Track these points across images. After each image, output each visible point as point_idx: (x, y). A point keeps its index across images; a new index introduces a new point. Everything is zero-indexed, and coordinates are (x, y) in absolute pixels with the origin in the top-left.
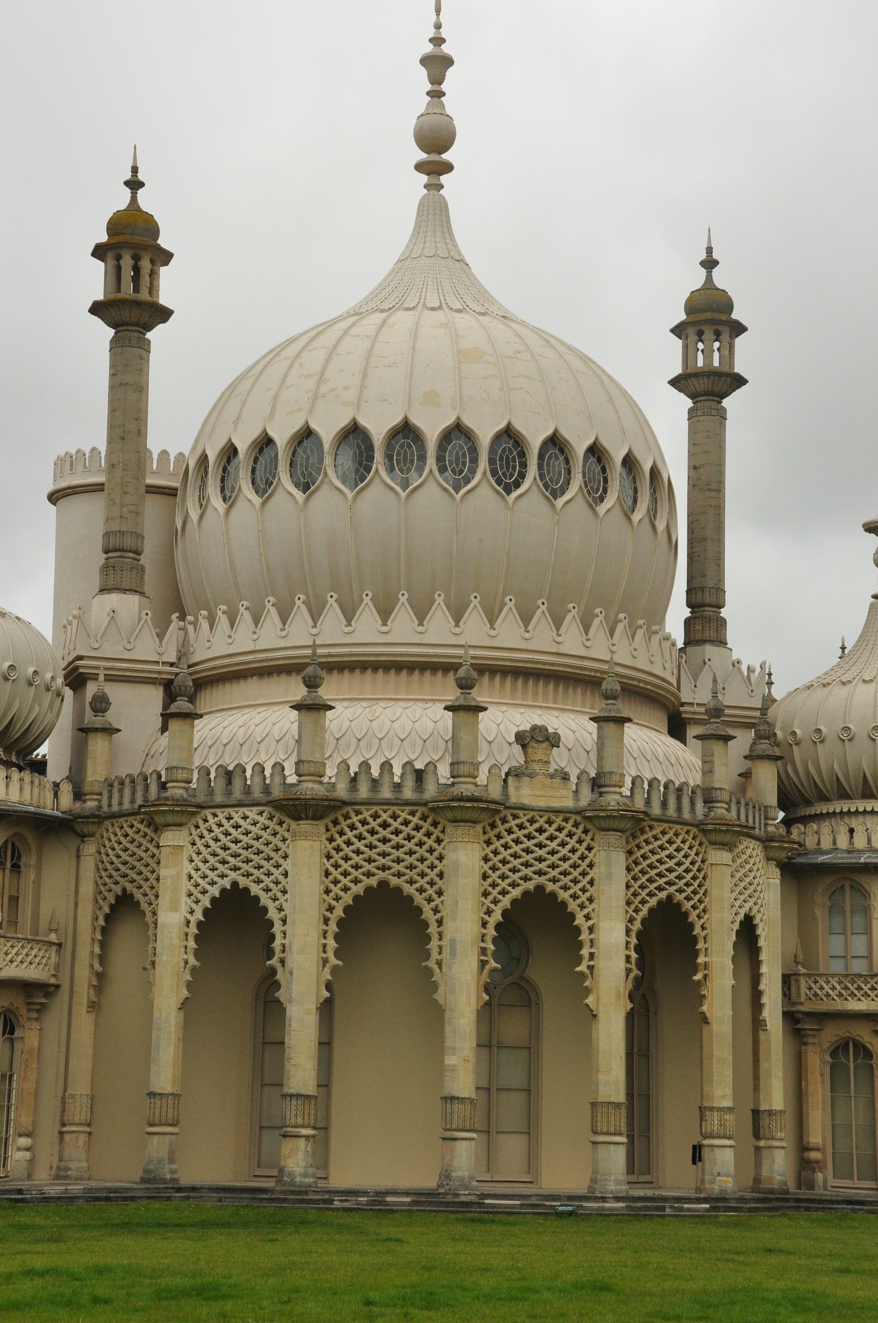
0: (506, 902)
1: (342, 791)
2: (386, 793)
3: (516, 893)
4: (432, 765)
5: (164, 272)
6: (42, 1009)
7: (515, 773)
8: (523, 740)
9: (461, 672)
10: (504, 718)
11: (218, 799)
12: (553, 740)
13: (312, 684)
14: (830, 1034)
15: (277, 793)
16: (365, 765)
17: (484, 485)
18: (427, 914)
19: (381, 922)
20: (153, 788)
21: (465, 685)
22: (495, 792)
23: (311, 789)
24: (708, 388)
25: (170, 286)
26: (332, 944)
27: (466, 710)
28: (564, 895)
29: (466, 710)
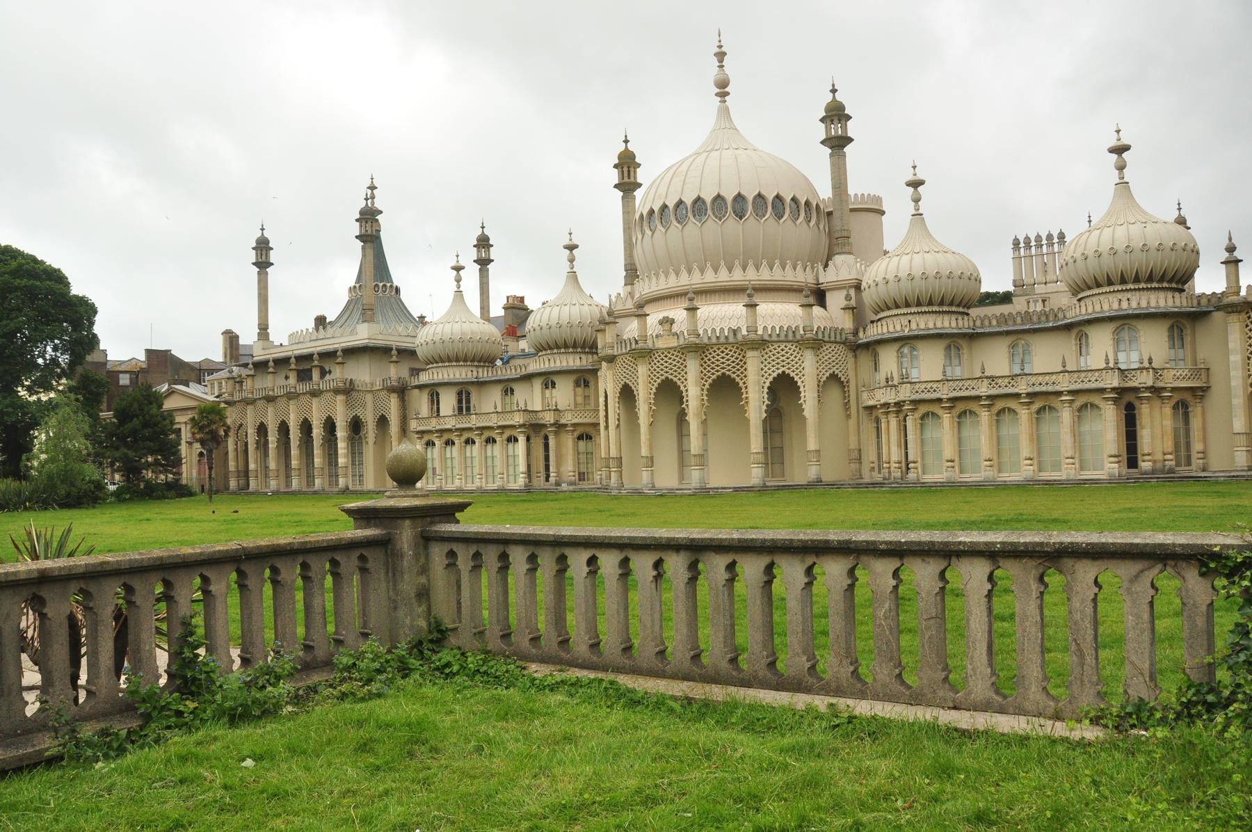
0: (710, 381)
19: (669, 391)
21: (691, 300)
27: (692, 310)
28: (733, 376)
29: (692, 310)
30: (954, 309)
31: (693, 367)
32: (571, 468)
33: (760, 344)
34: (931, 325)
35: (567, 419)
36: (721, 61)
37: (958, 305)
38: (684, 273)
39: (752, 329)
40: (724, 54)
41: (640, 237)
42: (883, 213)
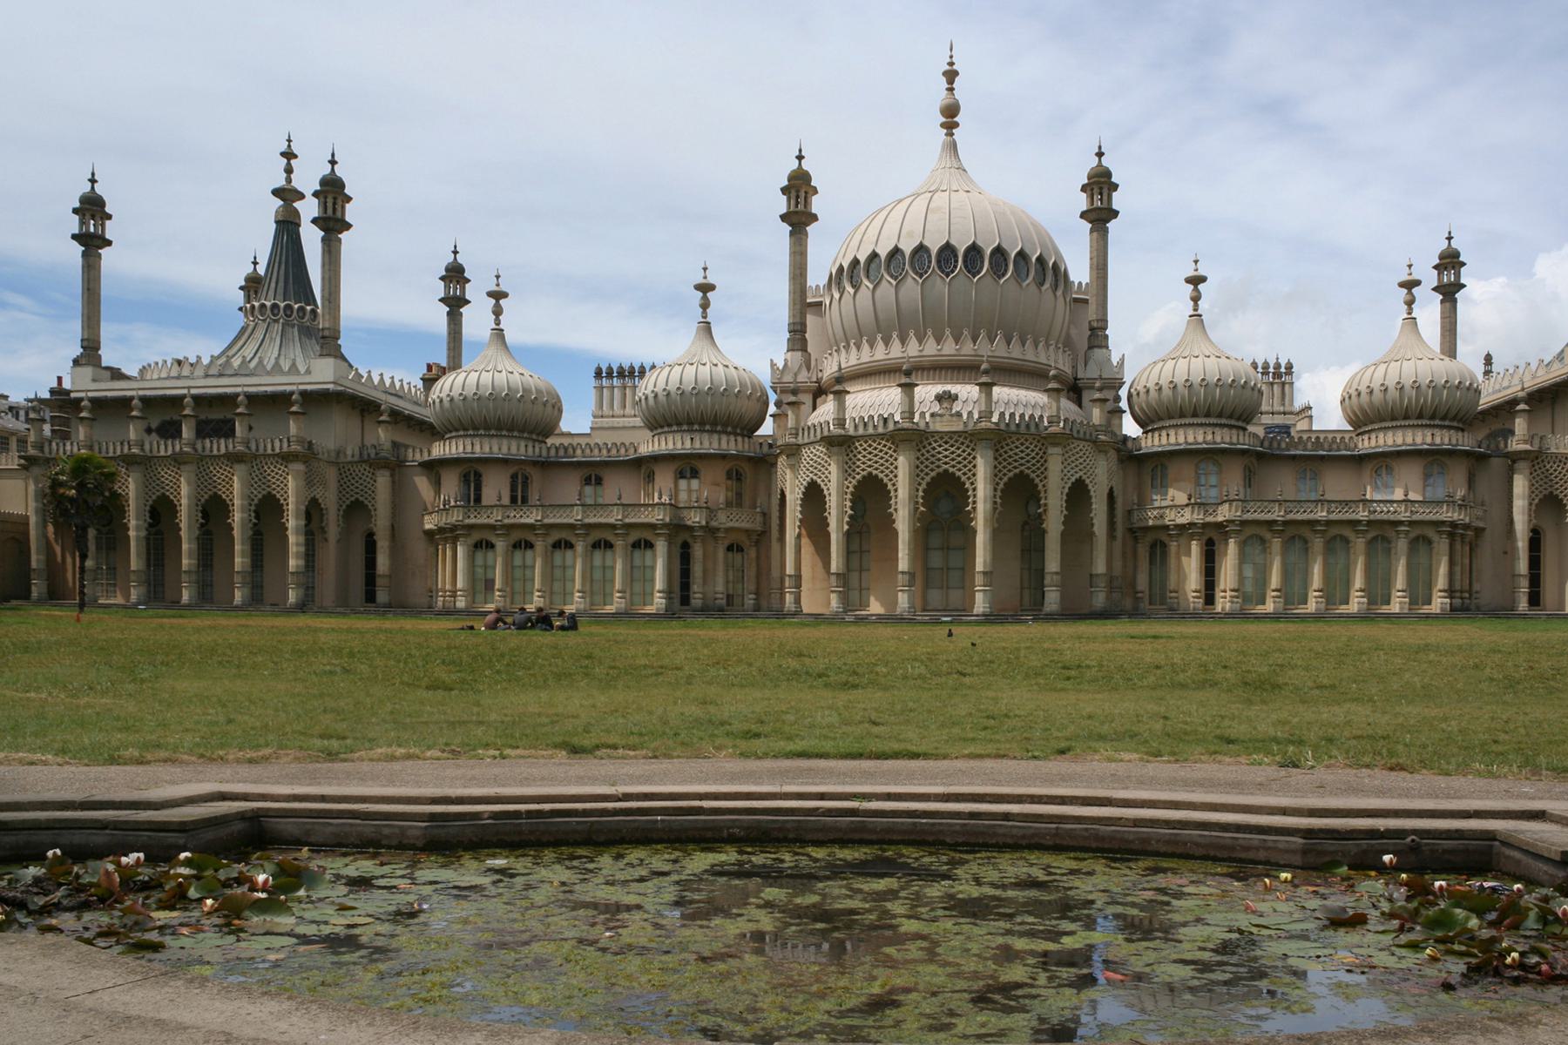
0: (928, 479)
1: (851, 432)
2: (871, 431)
3: (933, 474)
5: (814, 198)
6: (757, 543)
7: (932, 415)
8: (940, 398)
10: (926, 392)
12: (952, 398)
14: (1149, 538)
15: (826, 433)
17: (962, 276)
18: (890, 487)
22: (922, 426)
24: (1100, 216)
25: (817, 204)
26: (849, 504)
27: (908, 388)
29: (908, 388)
31: (903, 464)
32: (720, 588)
33: (998, 437)
34: (1200, 439)
35: (722, 520)
36: (951, 81)
37: (1238, 419)
38: (896, 343)
40: (956, 73)
41: (837, 296)
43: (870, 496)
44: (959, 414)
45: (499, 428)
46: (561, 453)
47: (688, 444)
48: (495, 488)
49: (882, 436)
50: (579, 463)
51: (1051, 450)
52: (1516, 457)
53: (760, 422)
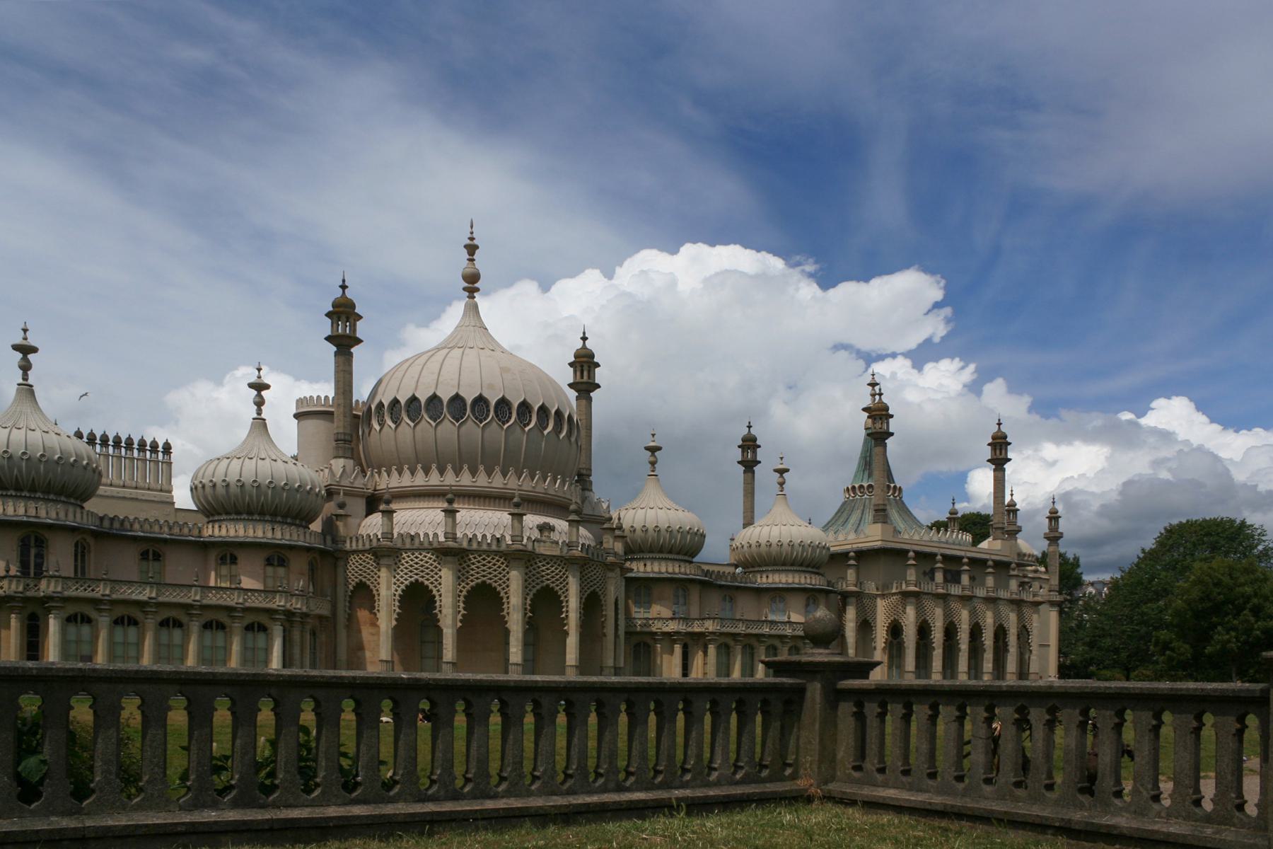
1: (465, 545)
2: (485, 547)
4: (503, 536)
7: (536, 540)
9: (515, 500)
11: (408, 546)
12: (552, 529)
13: (450, 502)
15: (435, 545)
16: (475, 535)
20: (375, 541)
22: (530, 547)
23: (451, 544)
30: (681, 557)
31: (515, 579)
39: (388, 535)
42: (297, 416)
43: (483, 602)
44: (557, 543)
45: (59, 493)
46: (117, 525)
47: (251, 533)
48: (60, 557)
49: (496, 553)
50: (135, 538)
51: (610, 574)
52: (845, 596)
53: (312, 520)
